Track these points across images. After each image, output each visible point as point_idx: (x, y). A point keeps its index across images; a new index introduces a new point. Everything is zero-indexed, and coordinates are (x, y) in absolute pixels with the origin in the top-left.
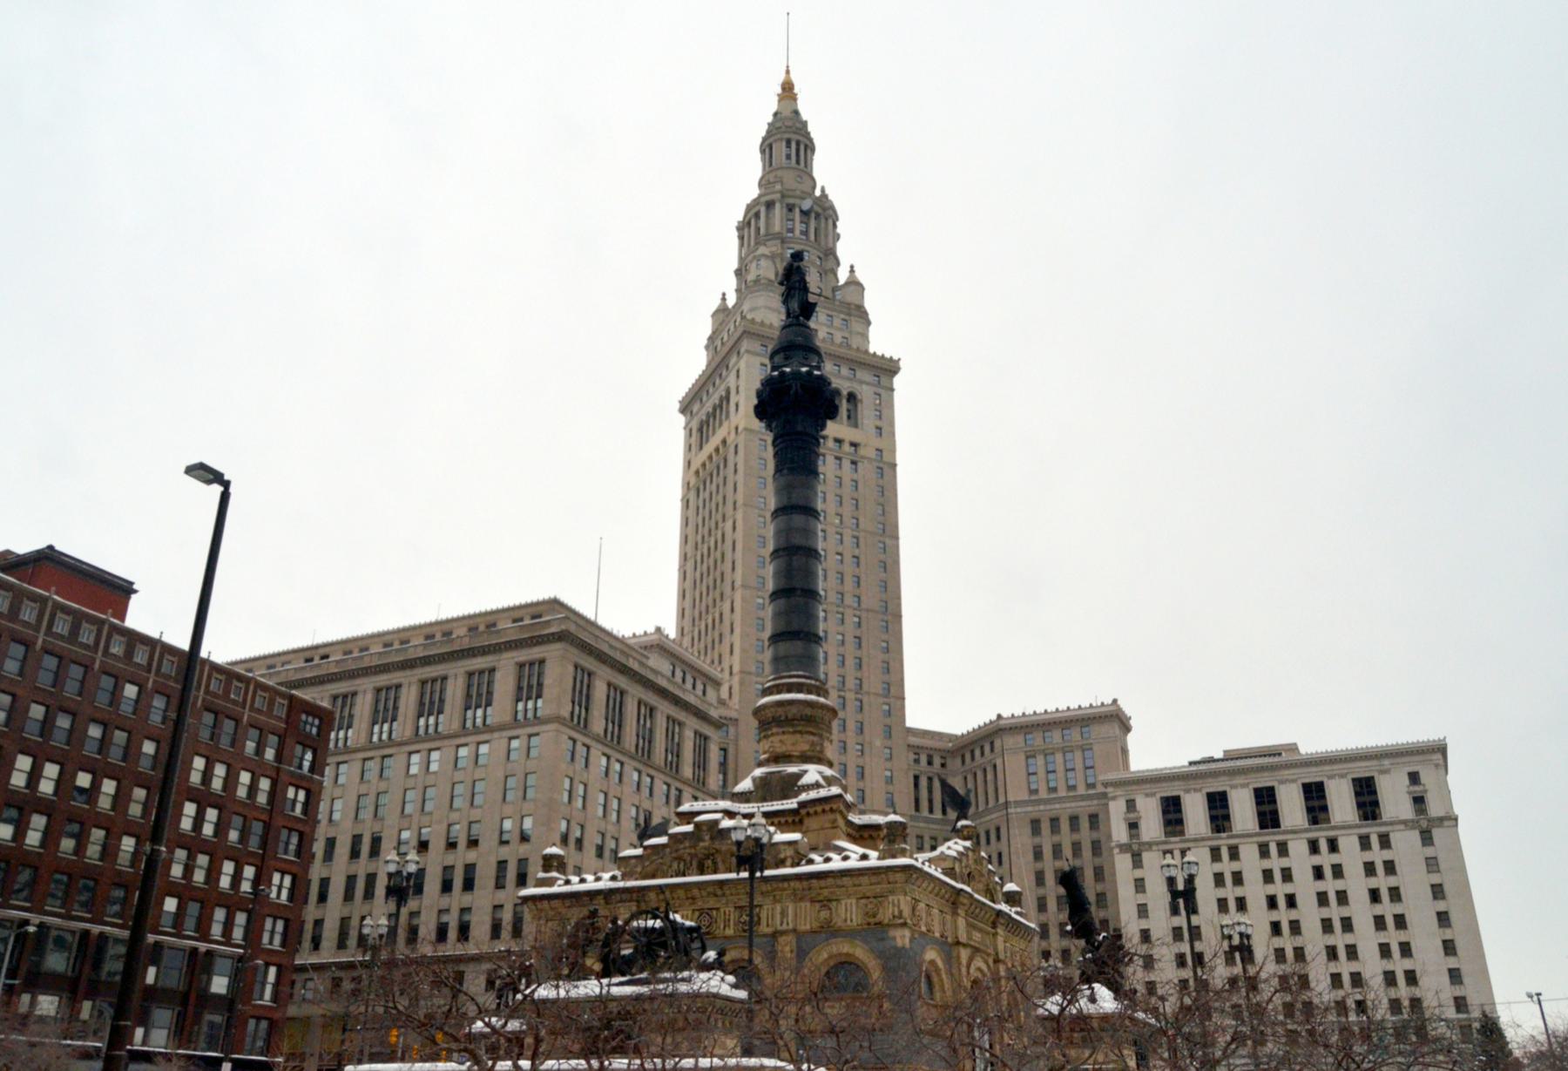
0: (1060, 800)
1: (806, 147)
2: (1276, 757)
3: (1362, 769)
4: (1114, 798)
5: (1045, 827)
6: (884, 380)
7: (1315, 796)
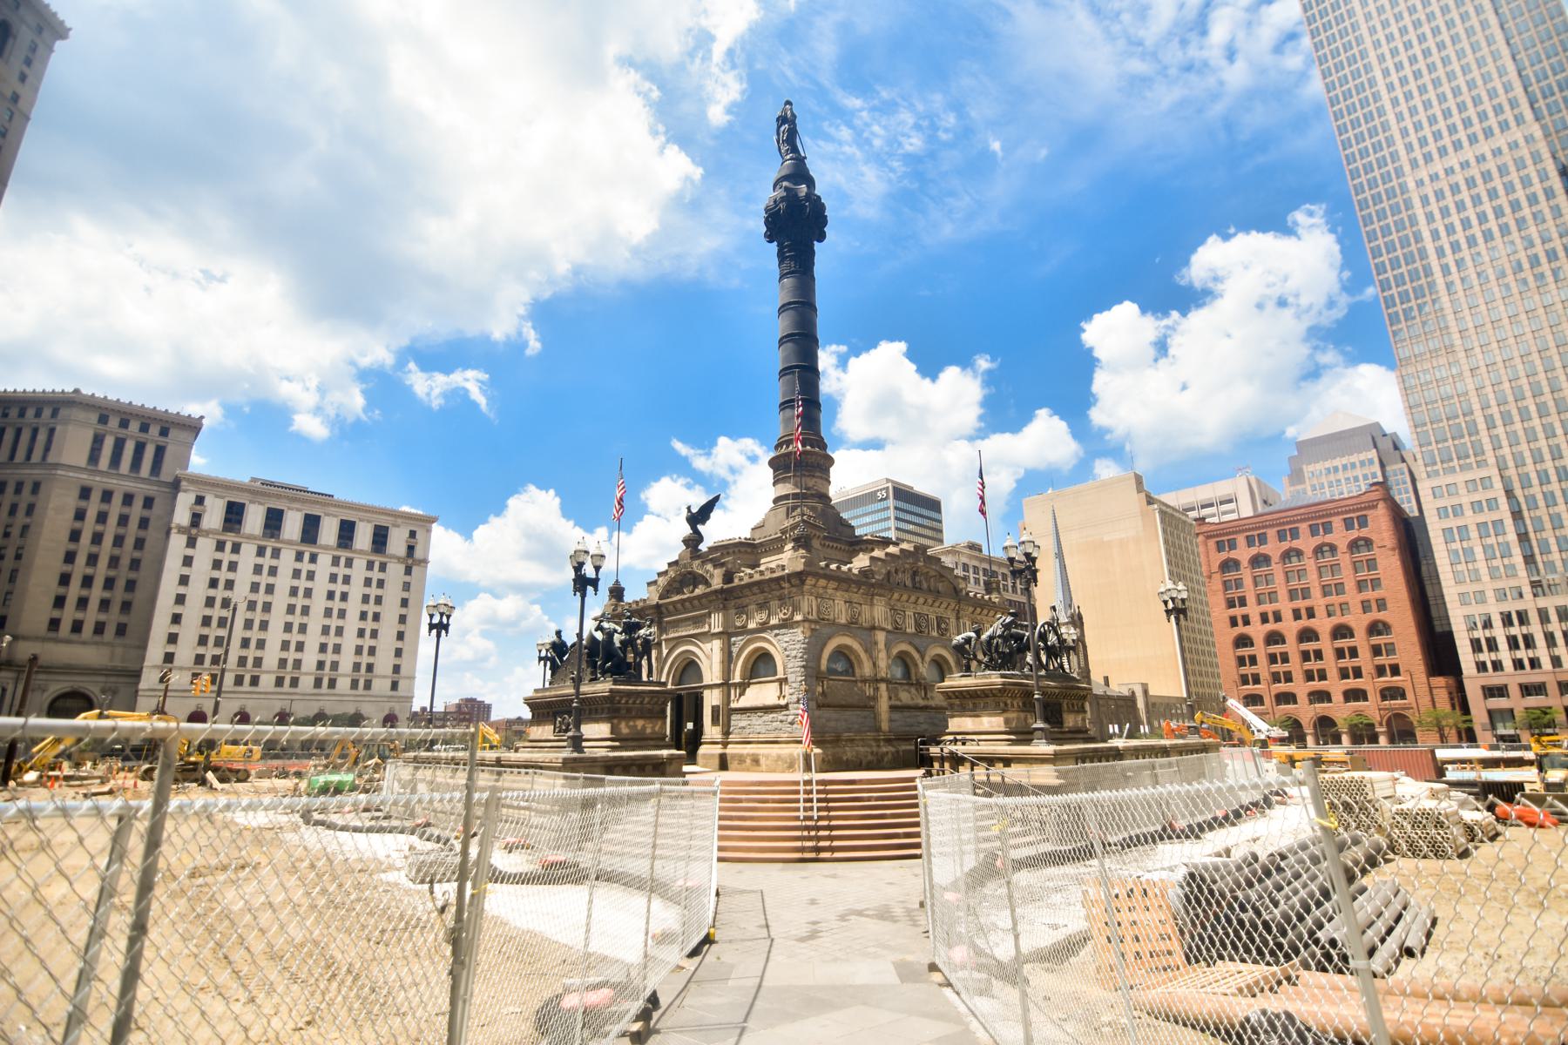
0: (101, 473)
2: (326, 499)
3: (383, 521)
5: (96, 496)
7: (347, 531)
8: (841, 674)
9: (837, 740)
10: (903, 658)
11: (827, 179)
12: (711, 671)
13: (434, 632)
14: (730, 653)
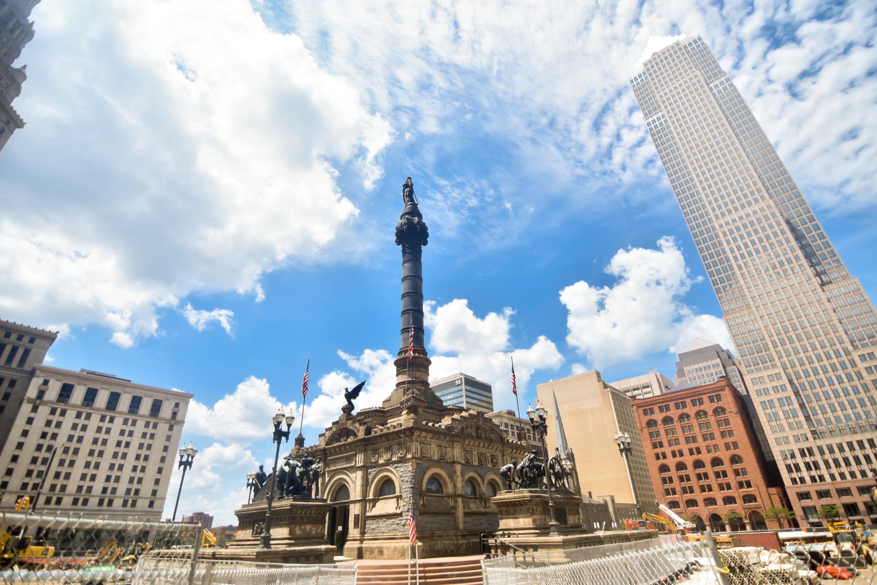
3: (159, 397)
4: (38, 377)
6: (11, 125)
7: (136, 402)
8: (434, 492)
9: (432, 536)
10: (471, 482)
11: (429, 216)
12: (355, 493)
13: (182, 467)
14: (367, 479)
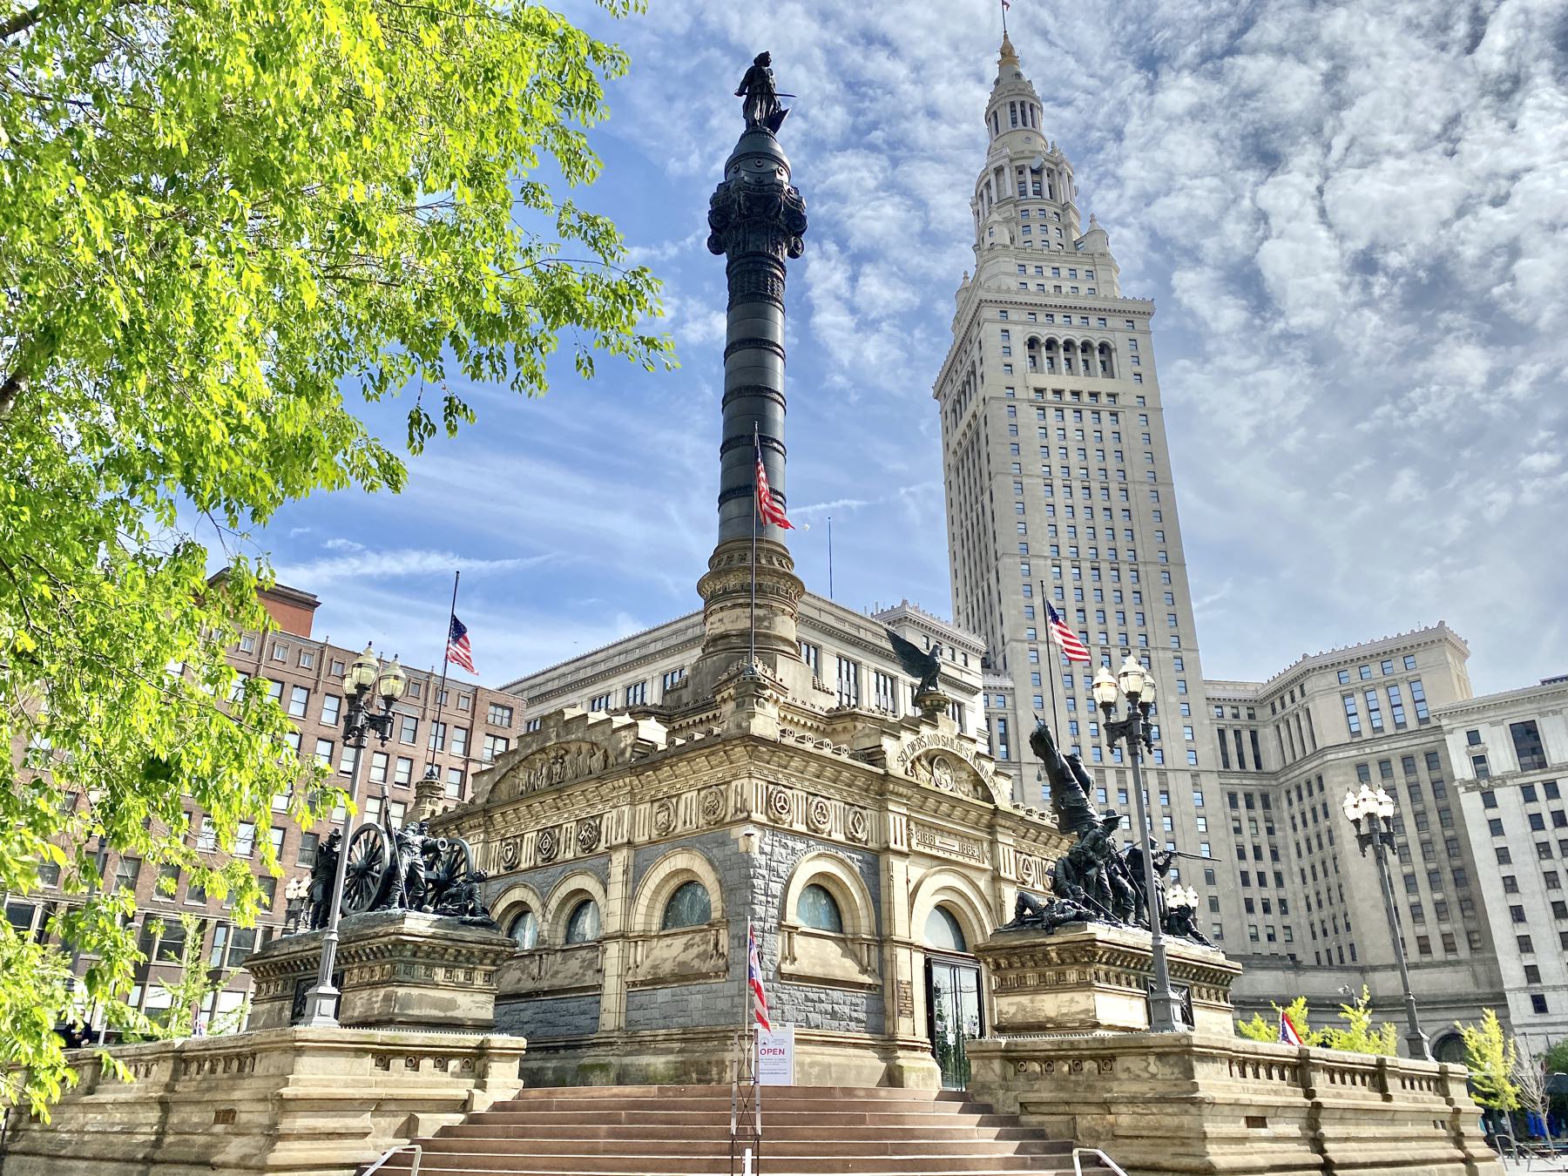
1: (1032, 106)
4: (1451, 732)
